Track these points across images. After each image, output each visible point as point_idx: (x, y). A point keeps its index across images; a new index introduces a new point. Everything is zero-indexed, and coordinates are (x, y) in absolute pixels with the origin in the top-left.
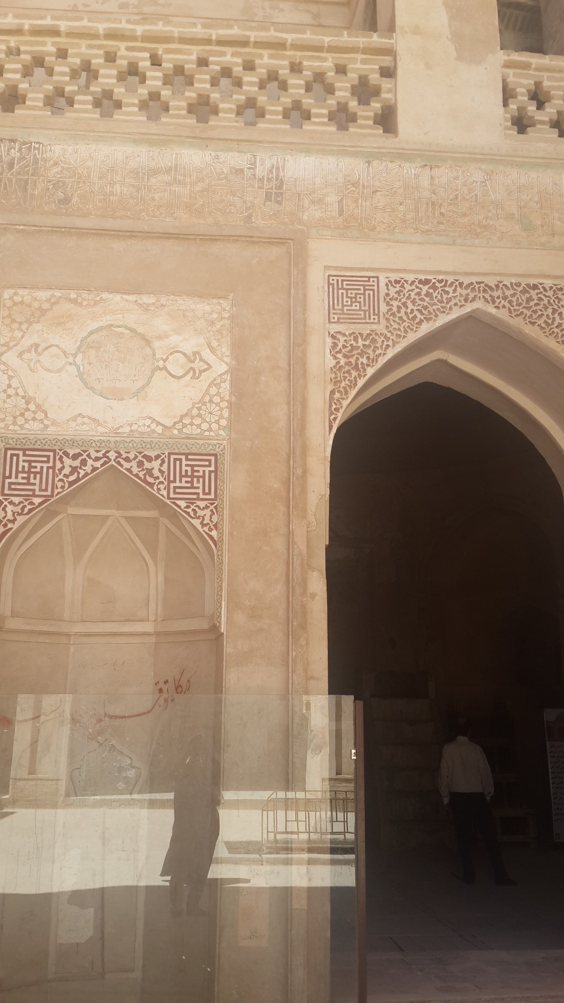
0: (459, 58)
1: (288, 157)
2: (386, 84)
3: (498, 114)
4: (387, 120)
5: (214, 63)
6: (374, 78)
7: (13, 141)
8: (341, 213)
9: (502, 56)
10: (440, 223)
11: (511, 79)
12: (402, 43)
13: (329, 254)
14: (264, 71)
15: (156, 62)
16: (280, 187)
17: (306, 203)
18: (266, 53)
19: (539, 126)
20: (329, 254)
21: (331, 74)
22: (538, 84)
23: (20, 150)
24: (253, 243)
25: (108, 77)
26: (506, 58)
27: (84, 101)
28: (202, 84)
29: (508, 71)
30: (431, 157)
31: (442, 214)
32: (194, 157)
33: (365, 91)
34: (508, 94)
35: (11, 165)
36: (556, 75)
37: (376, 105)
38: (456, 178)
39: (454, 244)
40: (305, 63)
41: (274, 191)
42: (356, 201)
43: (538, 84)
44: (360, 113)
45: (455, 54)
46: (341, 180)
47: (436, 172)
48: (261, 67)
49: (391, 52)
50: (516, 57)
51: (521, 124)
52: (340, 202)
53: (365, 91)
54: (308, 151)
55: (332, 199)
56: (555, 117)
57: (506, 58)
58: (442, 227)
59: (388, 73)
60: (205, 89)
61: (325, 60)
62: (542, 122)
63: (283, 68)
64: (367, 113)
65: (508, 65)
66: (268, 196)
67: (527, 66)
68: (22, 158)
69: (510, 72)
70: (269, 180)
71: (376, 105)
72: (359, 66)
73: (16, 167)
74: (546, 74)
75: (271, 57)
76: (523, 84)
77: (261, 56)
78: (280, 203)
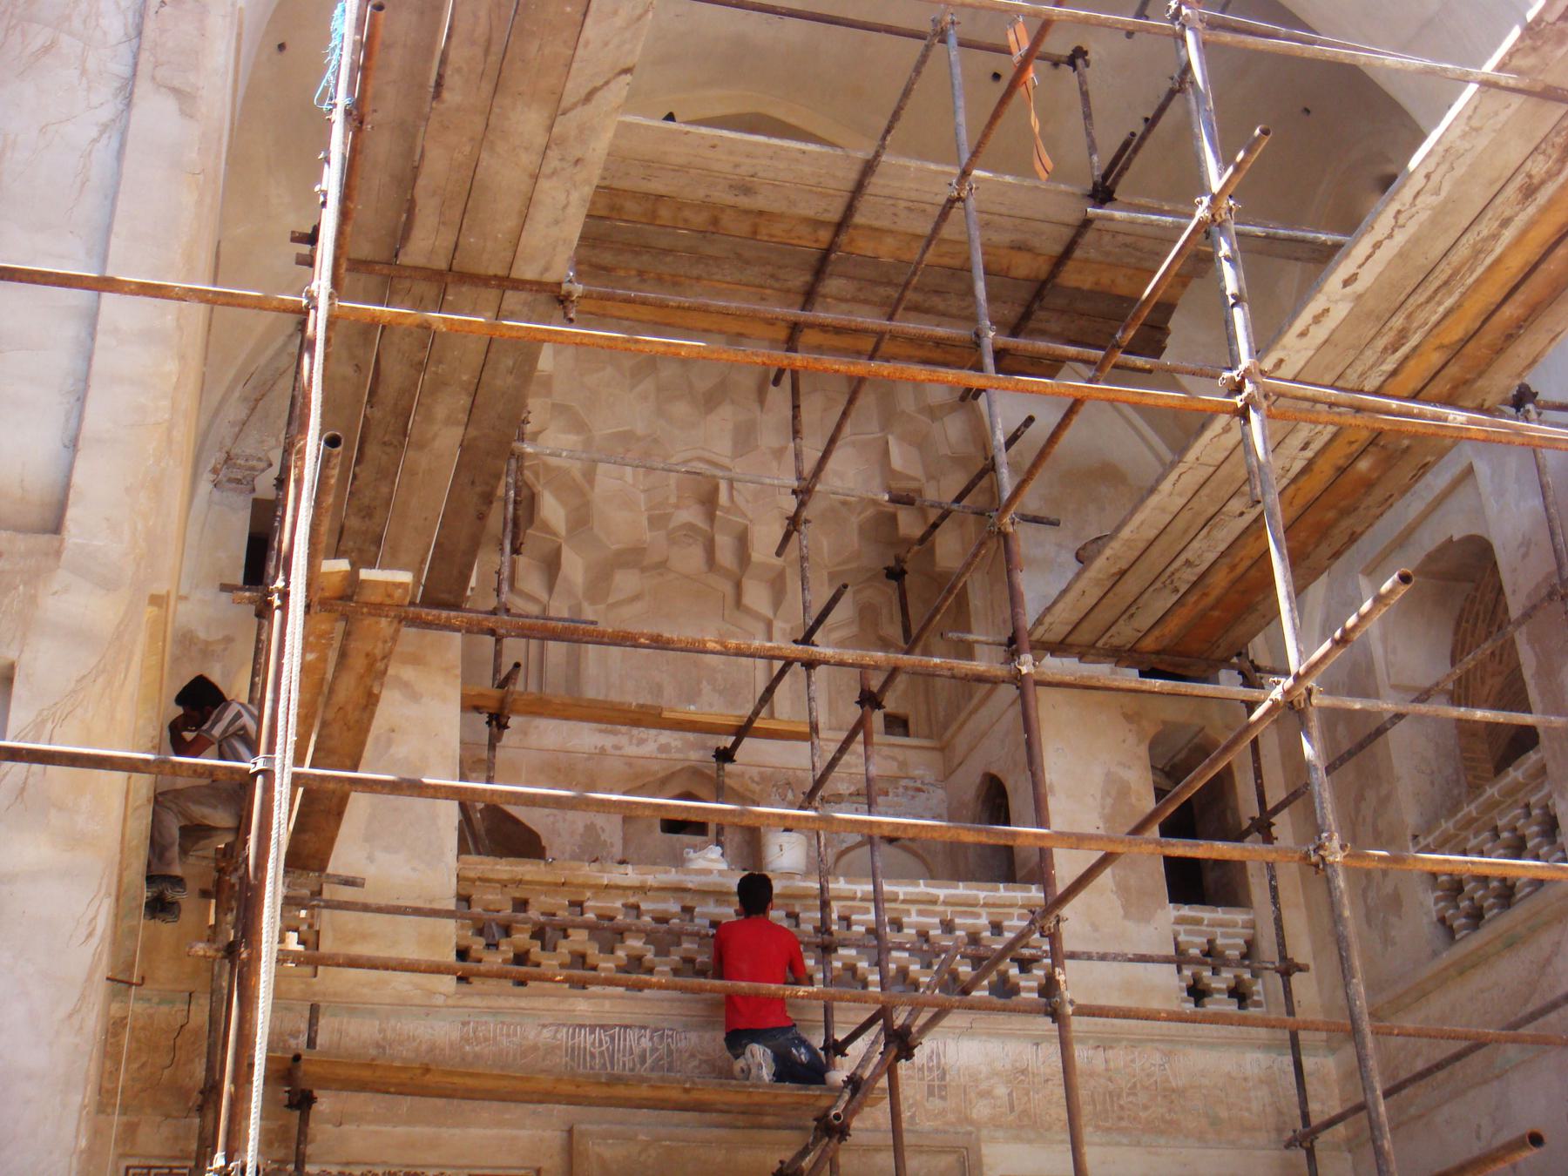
0: (1126, 916)
1: (949, 1041)
5: (858, 923)
7: (645, 1028)
8: (1012, 1109)
9: (1172, 911)
10: (1121, 1119)
11: (1182, 938)
14: (913, 931)
16: (943, 1078)
17: (973, 1095)
18: (913, 909)
19: (1217, 996)
21: (986, 934)
22: (1211, 942)
23: (651, 1039)
24: (921, 1152)
26: (1176, 913)
29: (1178, 928)
31: (1122, 1108)
35: (643, 1061)
36: (1230, 930)
38: (1133, 1061)
39: (1138, 1144)
40: (957, 921)
41: (936, 1083)
42: (1027, 1094)
43: (1211, 942)
44: (1022, 984)
45: (1121, 912)
46: (1008, 1066)
47: (1110, 1053)
48: (910, 926)
50: (1187, 911)
52: (1010, 1094)
55: (1001, 1091)
56: (1233, 984)
57: (1176, 913)
58: (1124, 1124)
60: (851, 957)
61: (978, 916)
62: (1219, 991)
63: (933, 927)
65: (1180, 921)
66: (931, 1092)
67: (1198, 922)
68: (654, 1050)
69: (1181, 928)
70: (930, 1069)
73: (649, 1061)
74: (1219, 930)
75: (920, 913)
77: (908, 913)
78: (943, 1098)
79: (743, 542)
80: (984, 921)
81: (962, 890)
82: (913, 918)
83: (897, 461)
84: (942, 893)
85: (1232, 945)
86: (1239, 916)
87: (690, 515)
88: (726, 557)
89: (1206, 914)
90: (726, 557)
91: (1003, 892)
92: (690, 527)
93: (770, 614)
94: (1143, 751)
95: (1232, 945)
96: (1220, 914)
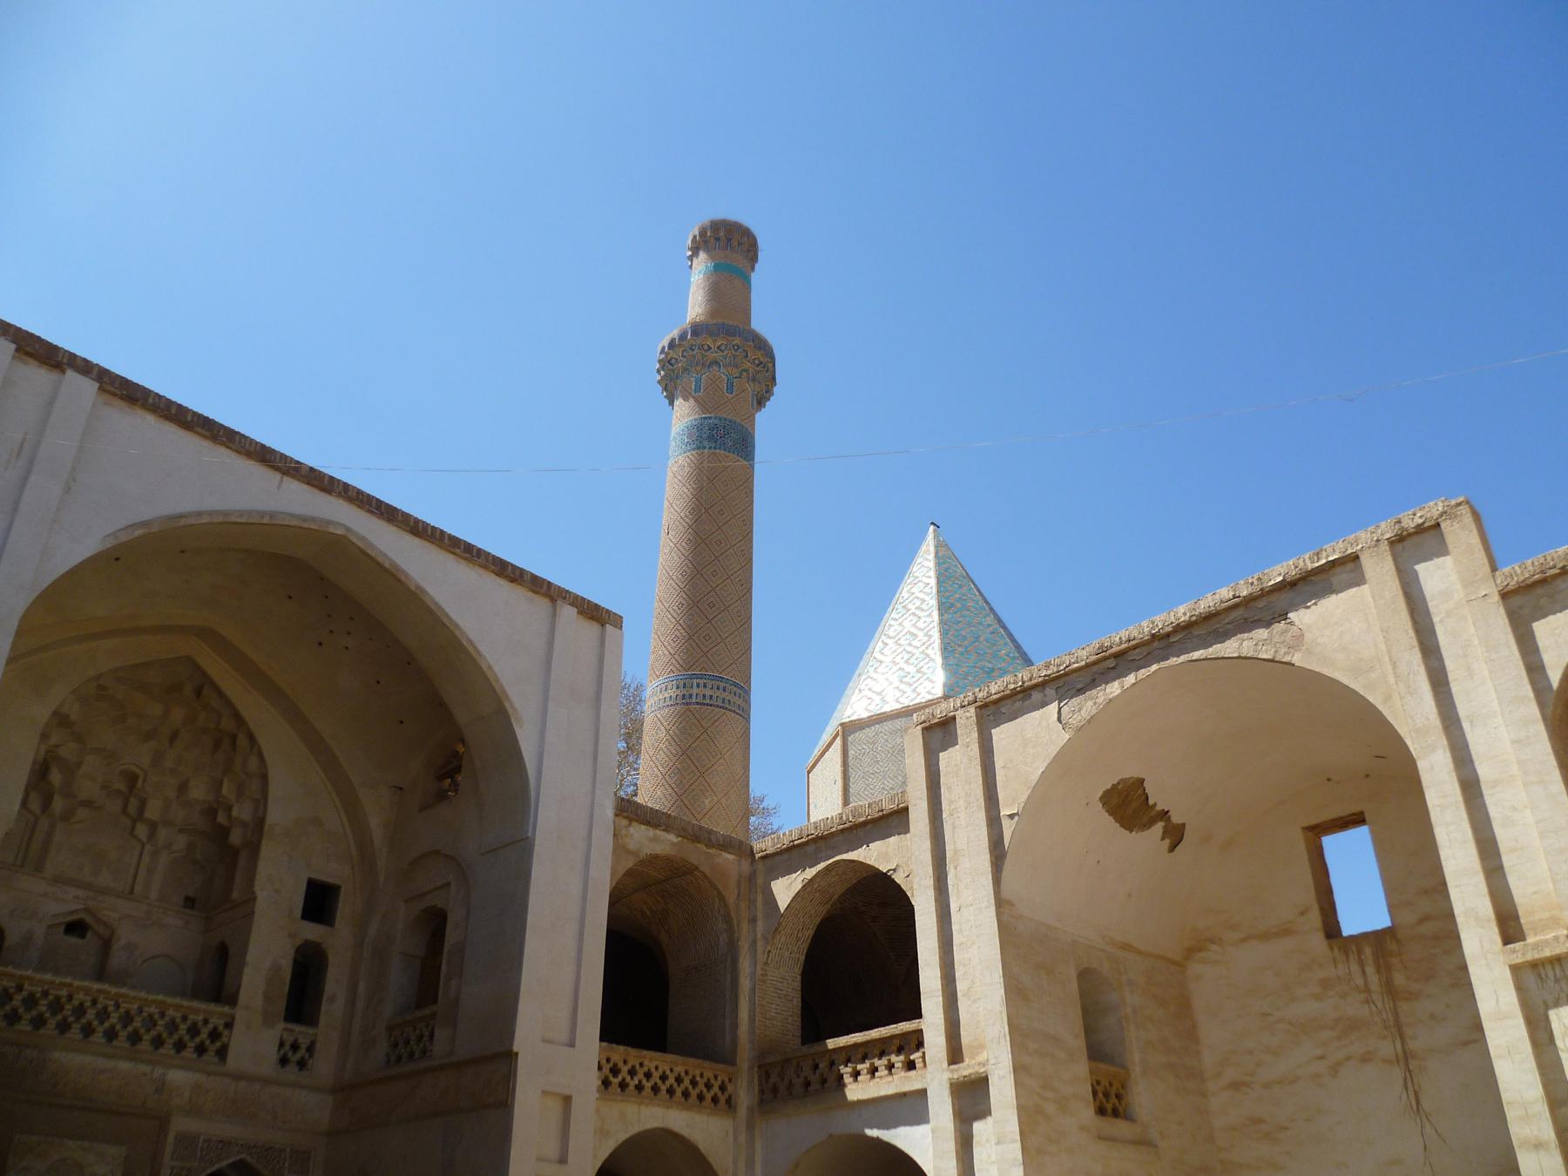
2: (226, 1033)
3: (272, 1053)
4: (222, 1053)
6: (221, 1028)
9: (282, 1025)
12: (240, 1013)
13: (181, 1124)
15: (117, 1006)
20: (181, 1124)
25: (91, 1014)
27: (76, 1028)
28: (137, 1023)
30: (237, 1077)
32: (125, 1066)
33: (215, 1035)
34: (282, 1044)
37: (218, 1044)
49: (233, 1018)
50: (290, 1026)
51: (284, 1061)
53: (215, 1035)
54: (181, 1067)
59: (229, 1026)
64: (213, 1048)
67: (292, 1031)
71: (218, 1044)
72: (216, 1021)
76: (289, 1039)
79: (143, 804)
80: (201, 1017)
81: (195, 1004)
82: (171, 1012)
83: (225, 791)
84: (185, 1003)
85: (304, 1042)
86: (310, 1030)
87: (121, 786)
88: (132, 810)
89: (298, 1028)
90: (132, 810)
91: (212, 1007)
92: (119, 792)
93: (144, 839)
94: (292, 951)
95: (304, 1042)
96: (303, 1029)
